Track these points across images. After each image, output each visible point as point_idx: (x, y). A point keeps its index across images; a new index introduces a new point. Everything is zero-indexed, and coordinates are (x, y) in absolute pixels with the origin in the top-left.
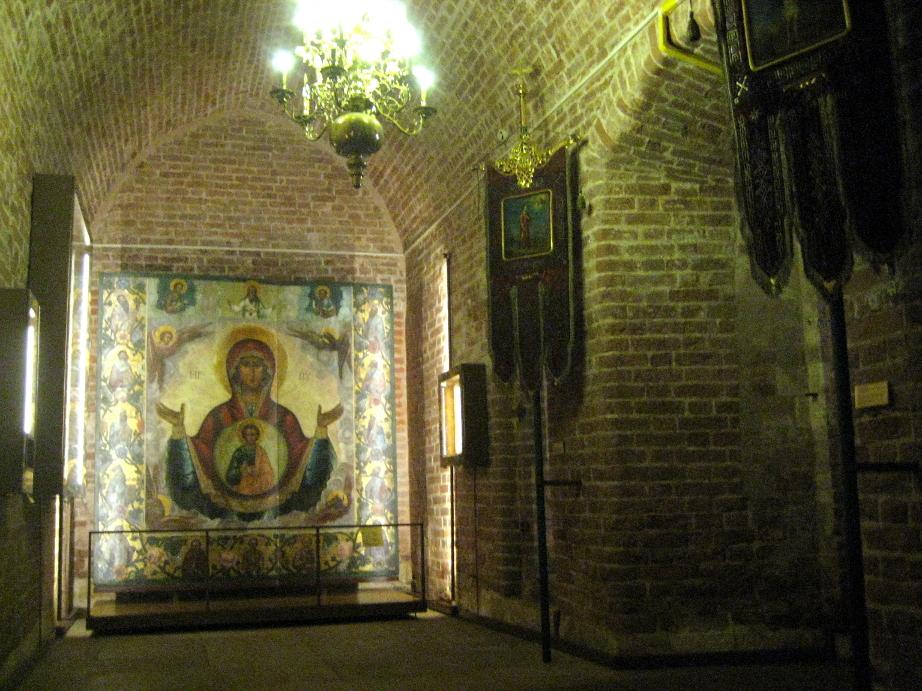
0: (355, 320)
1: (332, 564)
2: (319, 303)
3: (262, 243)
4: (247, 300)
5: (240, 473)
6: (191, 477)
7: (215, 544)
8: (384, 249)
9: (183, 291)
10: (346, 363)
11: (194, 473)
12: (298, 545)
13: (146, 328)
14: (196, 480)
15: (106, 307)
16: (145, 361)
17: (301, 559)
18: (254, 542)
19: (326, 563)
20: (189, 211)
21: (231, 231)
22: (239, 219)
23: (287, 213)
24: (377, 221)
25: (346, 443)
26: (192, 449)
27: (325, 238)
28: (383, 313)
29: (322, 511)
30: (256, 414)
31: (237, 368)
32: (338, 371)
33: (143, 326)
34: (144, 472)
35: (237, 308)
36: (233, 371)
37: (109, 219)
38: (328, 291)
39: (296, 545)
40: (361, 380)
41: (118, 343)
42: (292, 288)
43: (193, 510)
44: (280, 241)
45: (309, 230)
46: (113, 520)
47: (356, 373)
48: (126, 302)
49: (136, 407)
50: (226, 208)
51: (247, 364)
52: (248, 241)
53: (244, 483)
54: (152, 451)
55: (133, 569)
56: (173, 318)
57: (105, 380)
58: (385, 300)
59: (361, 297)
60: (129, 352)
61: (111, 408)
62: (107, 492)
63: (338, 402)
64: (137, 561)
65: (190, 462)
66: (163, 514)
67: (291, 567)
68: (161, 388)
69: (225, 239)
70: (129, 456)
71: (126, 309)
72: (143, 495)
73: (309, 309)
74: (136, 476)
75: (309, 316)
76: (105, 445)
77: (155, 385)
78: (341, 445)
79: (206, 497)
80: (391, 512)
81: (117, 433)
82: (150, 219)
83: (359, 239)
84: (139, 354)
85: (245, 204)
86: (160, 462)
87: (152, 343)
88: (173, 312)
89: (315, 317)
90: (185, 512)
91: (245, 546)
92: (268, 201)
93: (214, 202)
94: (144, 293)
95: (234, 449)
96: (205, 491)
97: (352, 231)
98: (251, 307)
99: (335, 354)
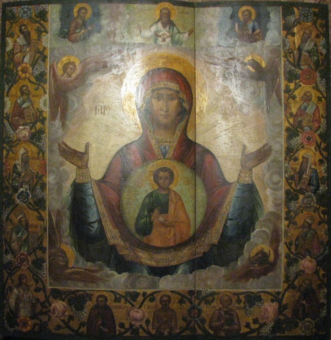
1: (254, 326)
4: (160, 25)
5: (151, 223)
6: (96, 225)
7: (123, 300)
11: (100, 221)
12: (216, 304)
13: (48, 60)
14: (102, 229)
17: (219, 319)
18: (165, 298)
25: (274, 189)
26: (97, 194)
28: (317, 36)
30: (170, 154)
38: (253, 11)
39: (214, 304)
40: (291, 114)
42: (211, 10)
55: (38, 322)
58: (319, 21)
59: (292, 19)
61: (13, 148)
63: (265, 142)
65: (95, 209)
66: (66, 266)
67: (207, 327)
68: (63, 125)
77: (57, 123)
79: (113, 248)
80: (323, 270)
86: (64, 208)
87: (55, 75)
90: (89, 264)
94: (46, 21)
95: (144, 195)
96: (112, 242)
98: (164, 31)
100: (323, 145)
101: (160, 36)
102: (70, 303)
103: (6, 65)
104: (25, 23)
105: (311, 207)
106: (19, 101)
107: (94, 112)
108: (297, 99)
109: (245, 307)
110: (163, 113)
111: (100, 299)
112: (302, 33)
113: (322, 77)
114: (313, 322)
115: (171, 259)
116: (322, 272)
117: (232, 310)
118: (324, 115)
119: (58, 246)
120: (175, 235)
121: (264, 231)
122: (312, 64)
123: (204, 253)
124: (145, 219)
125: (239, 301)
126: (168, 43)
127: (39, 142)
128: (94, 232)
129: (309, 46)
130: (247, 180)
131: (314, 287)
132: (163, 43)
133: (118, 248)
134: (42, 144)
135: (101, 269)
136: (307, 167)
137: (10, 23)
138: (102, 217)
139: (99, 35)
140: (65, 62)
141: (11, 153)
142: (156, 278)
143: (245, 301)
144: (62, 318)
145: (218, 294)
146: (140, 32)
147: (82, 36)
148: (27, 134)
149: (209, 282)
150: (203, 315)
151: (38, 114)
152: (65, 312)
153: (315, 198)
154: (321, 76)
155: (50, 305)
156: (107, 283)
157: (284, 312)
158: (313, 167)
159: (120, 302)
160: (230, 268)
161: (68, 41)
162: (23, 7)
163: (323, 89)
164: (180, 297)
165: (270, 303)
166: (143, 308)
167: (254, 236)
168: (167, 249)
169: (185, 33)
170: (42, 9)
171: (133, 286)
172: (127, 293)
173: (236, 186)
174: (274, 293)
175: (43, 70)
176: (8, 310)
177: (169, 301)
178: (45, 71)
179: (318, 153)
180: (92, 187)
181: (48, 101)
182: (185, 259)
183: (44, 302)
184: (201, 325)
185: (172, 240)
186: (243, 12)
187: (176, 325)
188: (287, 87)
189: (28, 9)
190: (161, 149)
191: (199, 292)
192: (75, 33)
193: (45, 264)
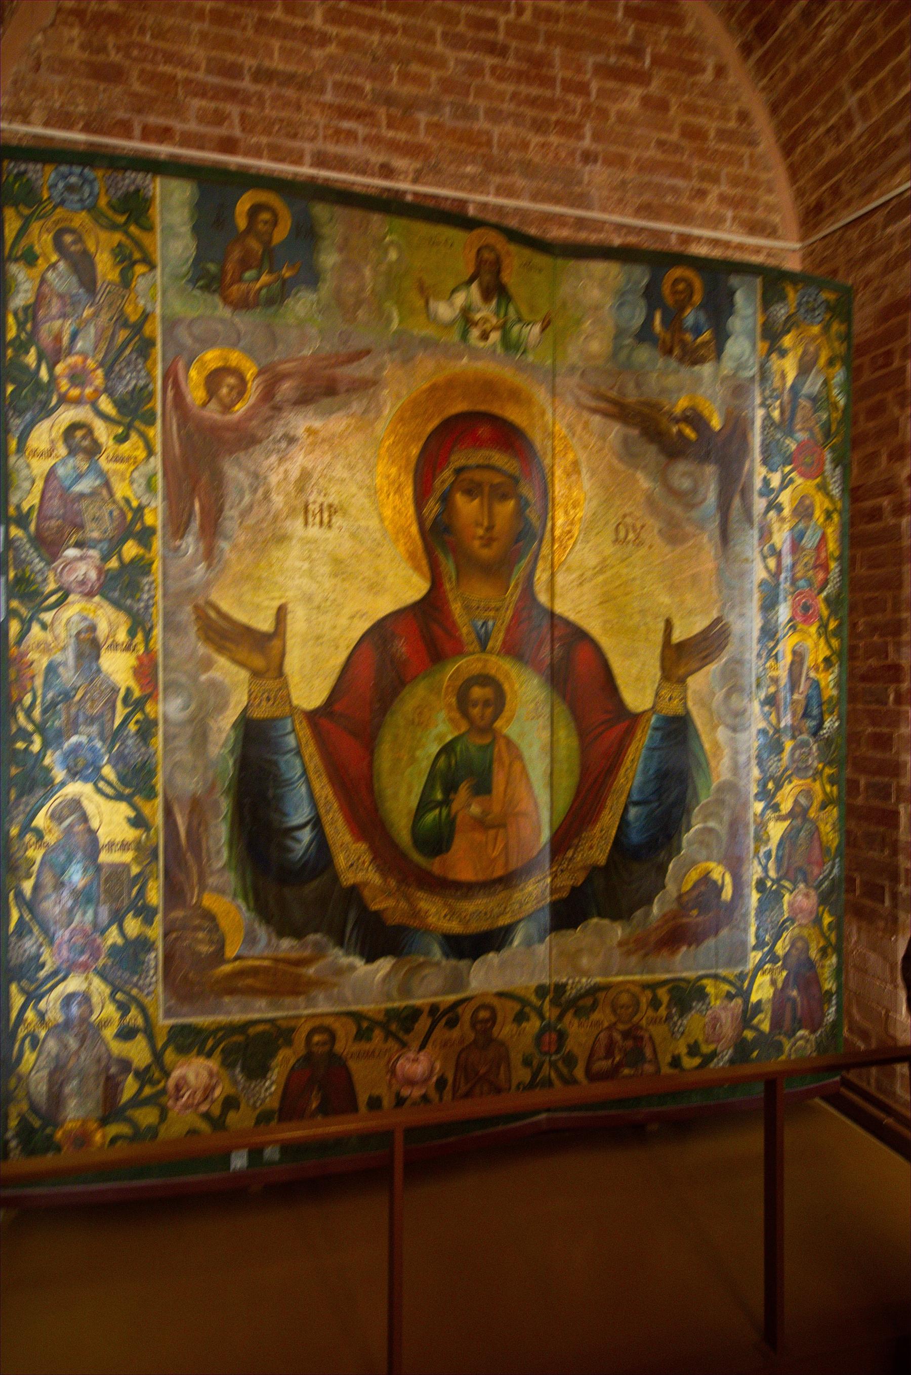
0: (764, 374)
2: (673, 320)
3: (472, 179)
4: (474, 288)
5: (451, 822)
6: (306, 835)
7: (378, 1034)
8: (754, 228)
9: (280, 234)
10: (737, 502)
11: (316, 822)
12: (603, 1016)
14: (321, 843)
15: (17, 270)
16: (156, 462)
17: (609, 1053)
18: (483, 1014)
19: (676, 1062)
20: (277, 63)
21: (391, 134)
22: (411, 106)
23: (532, 102)
24: (745, 151)
25: (734, 729)
26: (310, 750)
27: (624, 183)
28: (831, 363)
29: (666, 918)
30: (497, 641)
31: (446, 499)
32: (714, 526)
33: (150, 343)
34: (159, 820)
35: (444, 311)
36: (432, 508)
37: (45, 54)
38: (698, 284)
39: (596, 1016)
41: (64, 399)
42: (599, 267)
43: (312, 937)
44: (521, 182)
45: (588, 157)
46: (60, 975)
47: (765, 534)
48: (85, 253)
49: (128, 611)
50: (379, 75)
51: (471, 492)
52: (436, 170)
53: (460, 843)
54: (184, 756)
56: (244, 321)
57: (22, 521)
59: (781, 312)
60: (103, 432)
61: (47, 617)
62: (36, 888)
63: (715, 615)
64: (137, 1102)
65: (304, 789)
66: (218, 957)
68: (210, 554)
69: (377, 158)
70: (108, 771)
71: (88, 281)
72: (155, 895)
73: (644, 334)
74: (131, 834)
75: (644, 354)
76: (27, 737)
77: (190, 544)
78: (722, 734)
80: (831, 914)
81: (67, 696)
82: (168, 69)
83: (701, 194)
84: (134, 437)
85: (426, 60)
86: (212, 788)
88: (243, 304)
89: (660, 363)
90: (286, 943)
91: (463, 1031)
92: (489, 61)
93: (347, 44)
95: (434, 749)
96: (349, 878)
97: (682, 171)
98: (485, 312)
99: (710, 470)
100: (832, 625)
101: (476, 324)
102: (227, 1063)
103: (10, 352)
104: (76, 224)
105: (807, 768)
106: (61, 471)
107: (300, 521)
108: (786, 512)
109: (669, 1017)
110: (480, 532)
111: (316, 1038)
112: (800, 351)
113: (836, 462)
114: (813, 1037)
115: (496, 911)
116: (827, 919)
117: (637, 1027)
118: (837, 554)
119: (194, 901)
120: (506, 847)
121: (710, 830)
122: (817, 429)
123: (573, 889)
124: (437, 811)
125: (655, 1003)
126: (494, 344)
127: (132, 597)
128: (301, 853)
129: (813, 384)
130: (673, 708)
131: (814, 954)
132: (482, 344)
133: (367, 893)
134: (142, 604)
135: (320, 952)
136: (800, 674)
137: (19, 214)
138: (322, 811)
139: (314, 297)
140: (213, 366)
141: (36, 629)
142: (463, 964)
143: (670, 1000)
144: (204, 1108)
145: (607, 987)
146: (427, 303)
147: (264, 291)
148: (93, 575)
149: (585, 961)
150: (571, 1045)
151: (129, 516)
152: (213, 1088)
153: (815, 748)
154: (833, 461)
155: (167, 1074)
156: (336, 990)
157: (755, 1021)
158: (812, 674)
159: (369, 1039)
160: (634, 922)
161: (221, 305)
162: (64, 169)
163: (836, 492)
164: (517, 1007)
165: (726, 1002)
166: (429, 1045)
167: (690, 843)
168: (488, 886)
169: (534, 323)
170: (132, 188)
171: (405, 991)
172: (388, 1012)
173: (648, 720)
174: (732, 978)
175: (142, 383)
176: (24, 1106)
177: (493, 1019)
178: (146, 386)
179: (822, 642)
180: (294, 730)
181: (160, 475)
182: (529, 908)
183: (148, 1068)
184: (565, 1071)
185: (502, 861)
186: (676, 282)
187: (509, 1081)
188: (766, 482)
189: (85, 180)
190: (474, 626)
191: (560, 988)
192: (240, 280)
193: (153, 955)
